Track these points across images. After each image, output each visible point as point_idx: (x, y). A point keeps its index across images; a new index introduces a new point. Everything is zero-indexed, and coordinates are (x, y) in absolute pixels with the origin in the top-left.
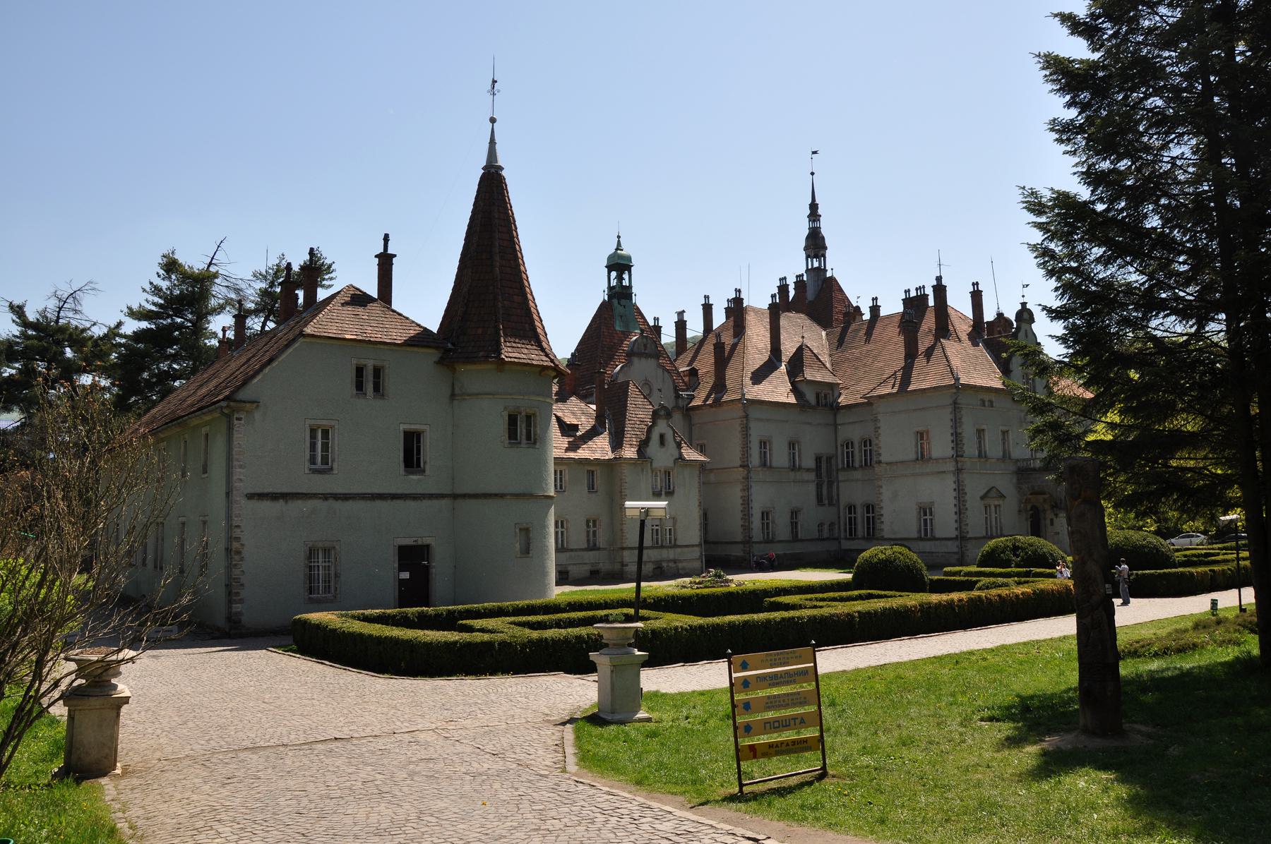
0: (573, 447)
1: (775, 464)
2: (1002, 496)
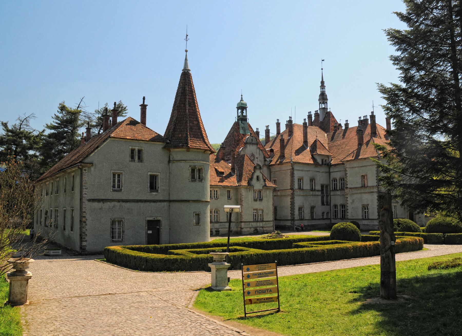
0: (222, 181)
1: (304, 188)
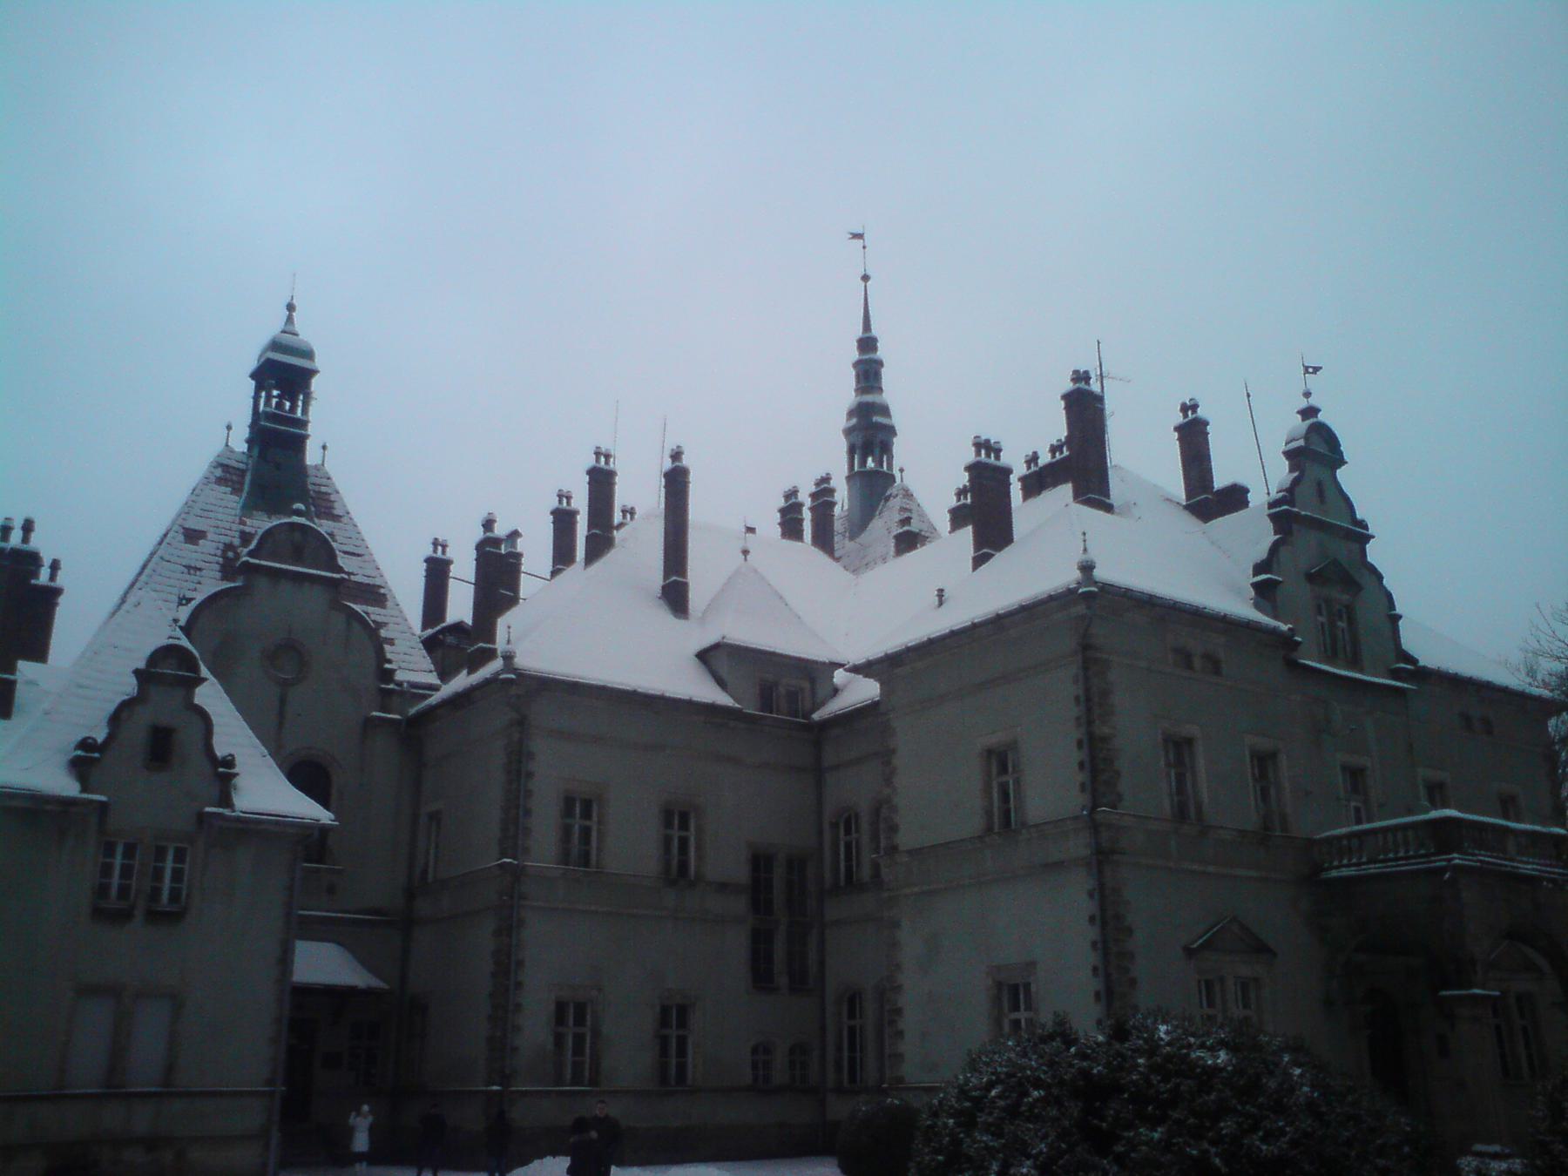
2: (1261, 949)
